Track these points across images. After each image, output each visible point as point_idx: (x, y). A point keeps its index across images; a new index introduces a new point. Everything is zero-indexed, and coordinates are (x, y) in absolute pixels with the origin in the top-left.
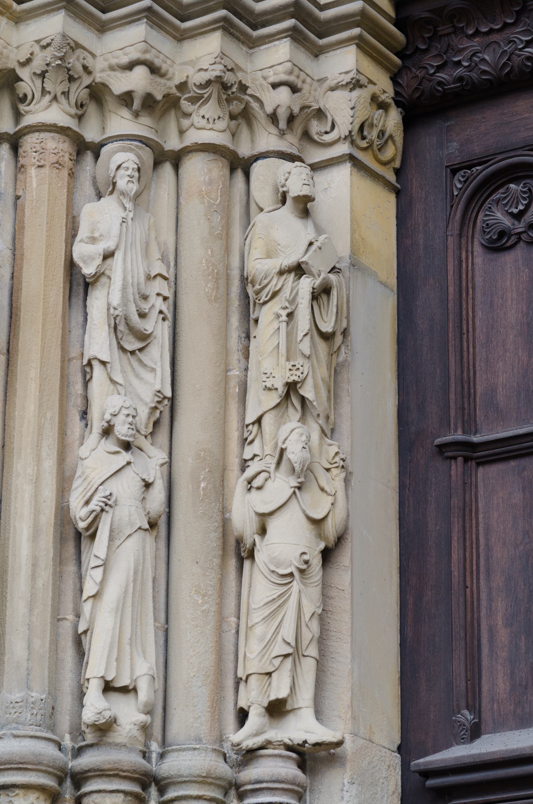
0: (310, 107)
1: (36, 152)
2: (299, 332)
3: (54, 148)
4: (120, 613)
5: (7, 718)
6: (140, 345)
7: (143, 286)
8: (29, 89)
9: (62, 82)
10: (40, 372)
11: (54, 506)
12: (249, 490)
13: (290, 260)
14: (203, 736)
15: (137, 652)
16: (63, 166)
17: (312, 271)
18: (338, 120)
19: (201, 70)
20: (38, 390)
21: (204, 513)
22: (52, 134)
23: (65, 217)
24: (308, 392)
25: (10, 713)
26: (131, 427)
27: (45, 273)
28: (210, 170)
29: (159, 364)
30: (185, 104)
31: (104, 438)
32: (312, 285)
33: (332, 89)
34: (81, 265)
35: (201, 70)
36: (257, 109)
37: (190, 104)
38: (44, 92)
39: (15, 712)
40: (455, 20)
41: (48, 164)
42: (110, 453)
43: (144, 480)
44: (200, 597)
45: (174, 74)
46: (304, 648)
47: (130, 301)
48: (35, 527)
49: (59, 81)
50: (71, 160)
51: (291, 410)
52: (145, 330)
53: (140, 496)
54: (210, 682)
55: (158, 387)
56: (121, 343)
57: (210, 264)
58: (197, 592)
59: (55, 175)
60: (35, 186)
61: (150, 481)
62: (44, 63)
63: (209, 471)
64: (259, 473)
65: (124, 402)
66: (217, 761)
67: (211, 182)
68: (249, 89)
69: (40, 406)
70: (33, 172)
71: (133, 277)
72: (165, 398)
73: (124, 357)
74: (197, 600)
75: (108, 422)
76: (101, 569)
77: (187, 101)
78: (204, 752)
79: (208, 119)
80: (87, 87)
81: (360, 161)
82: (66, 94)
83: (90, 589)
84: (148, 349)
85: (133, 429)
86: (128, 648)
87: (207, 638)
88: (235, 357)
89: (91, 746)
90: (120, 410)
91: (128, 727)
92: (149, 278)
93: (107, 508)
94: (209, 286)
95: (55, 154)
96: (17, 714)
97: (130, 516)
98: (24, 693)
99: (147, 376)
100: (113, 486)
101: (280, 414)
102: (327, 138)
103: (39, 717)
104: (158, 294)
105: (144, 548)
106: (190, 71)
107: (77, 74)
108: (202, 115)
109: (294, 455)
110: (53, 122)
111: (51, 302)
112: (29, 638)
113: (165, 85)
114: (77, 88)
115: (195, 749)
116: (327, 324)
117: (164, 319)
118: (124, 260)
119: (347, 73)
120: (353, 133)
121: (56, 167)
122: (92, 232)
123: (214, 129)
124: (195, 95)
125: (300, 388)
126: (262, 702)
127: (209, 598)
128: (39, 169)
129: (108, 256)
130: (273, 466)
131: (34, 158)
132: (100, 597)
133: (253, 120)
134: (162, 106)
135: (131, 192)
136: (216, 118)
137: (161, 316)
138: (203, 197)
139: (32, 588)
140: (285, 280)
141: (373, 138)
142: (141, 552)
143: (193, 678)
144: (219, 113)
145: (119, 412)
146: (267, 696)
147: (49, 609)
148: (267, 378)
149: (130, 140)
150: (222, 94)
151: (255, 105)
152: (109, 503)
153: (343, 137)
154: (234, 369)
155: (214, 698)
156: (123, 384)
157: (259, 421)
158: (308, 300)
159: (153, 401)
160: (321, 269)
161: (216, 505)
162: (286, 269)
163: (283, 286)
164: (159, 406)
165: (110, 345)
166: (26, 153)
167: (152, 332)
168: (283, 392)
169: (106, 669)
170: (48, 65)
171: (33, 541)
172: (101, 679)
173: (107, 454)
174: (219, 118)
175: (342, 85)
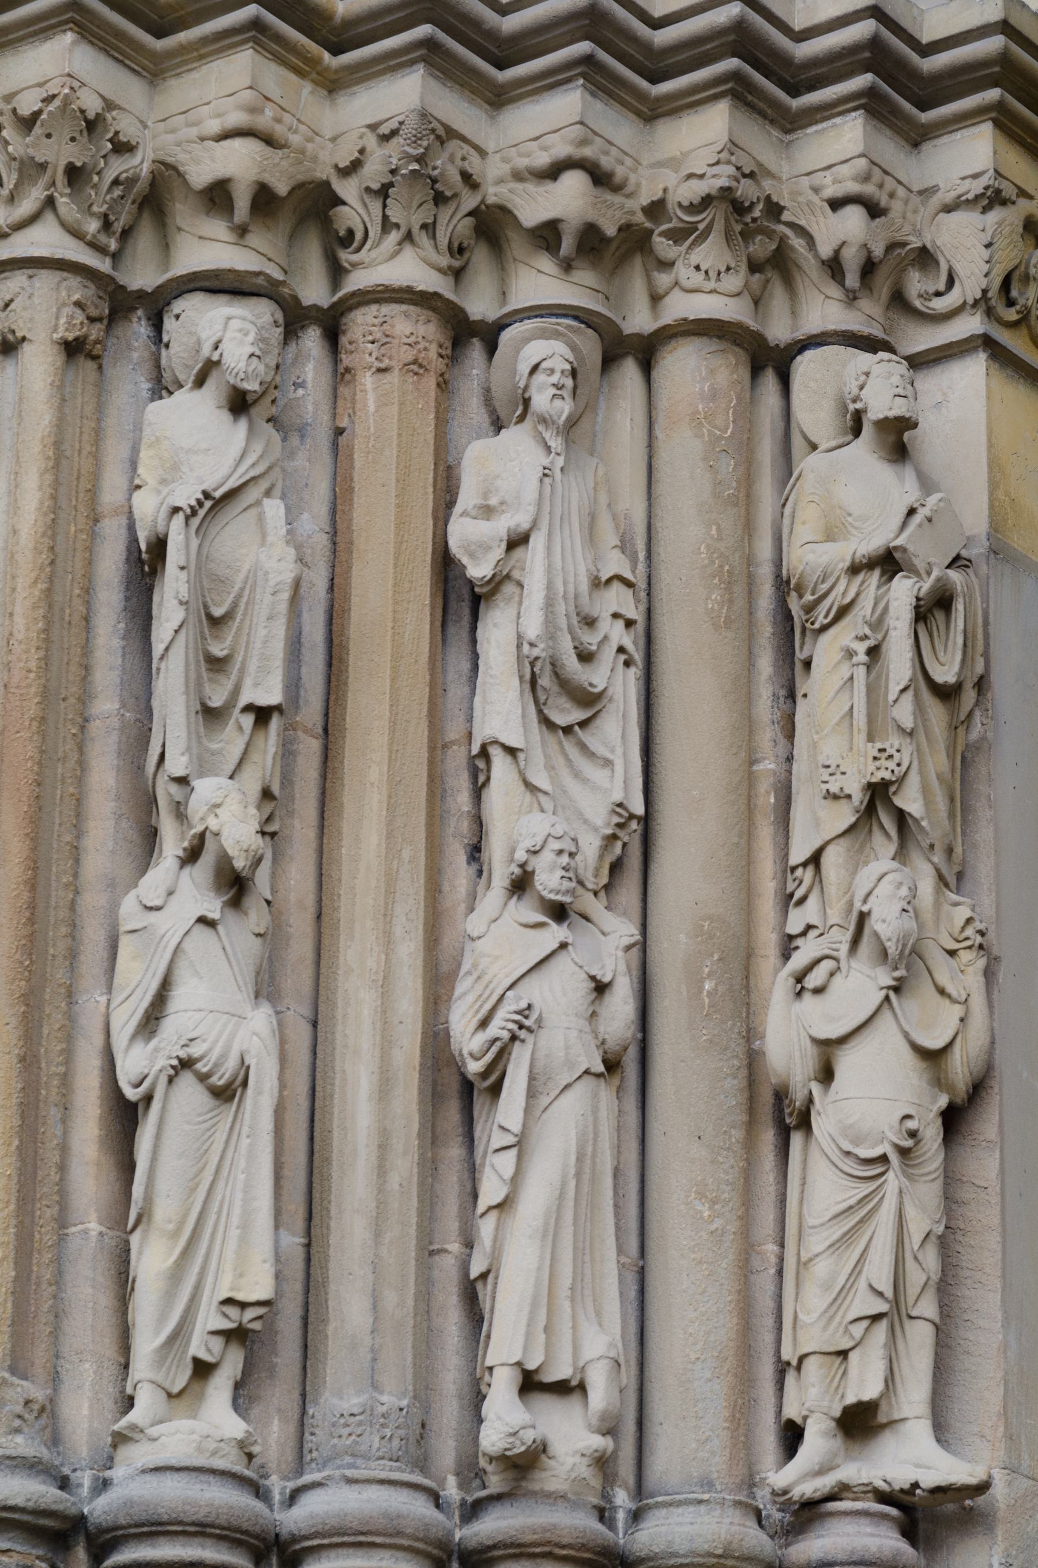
0: (904, 244)
1: (373, 342)
2: (891, 685)
3: (408, 333)
4: (550, 1238)
5: (335, 1446)
6: (579, 715)
7: (585, 600)
8: (358, 220)
9: (421, 205)
10: (389, 771)
11: (420, 1032)
12: (799, 994)
14: (715, 1475)
15: (586, 1315)
16: (426, 369)
17: (914, 565)
18: (960, 269)
19: (691, 176)
20: (385, 805)
21: (711, 1041)
22: (404, 307)
23: (432, 467)
24: (910, 801)
25: (340, 1436)
26: (567, 875)
27: (395, 578)
28: (712, 372)
29: (619, 751)
30: (663, 243)
31: (515, 898)
32: (915, 593)
33: (948, 209)
34: (465, 560)
35: (691, 176)
36: (802, 250)
37: (671, 242)
38: (387, 225)
39: (350, 1435)
42: (526, 926)
43: (593, 978)
44: (707, 1205)
45: (638, 185)
46: (910, 1302)
47: (561, 629)
48: (382, 1073)
49: (415, 204)
50: (441, 356)
51: (878, 837)
52: (591, 685)
53: (587, 1009)
54: (729, 1371)
55: (618, 796)
56: (546, 711)
57: (715, 555)
58: (701, 1195)
60: (372, 407)
61: (606, 979)
62: (387, 169)
63: (720, 960)
64: (818, 961)
66: (744, 1525)
67: (714, 395)
68: (786, 212)
69: (390, 835)
70: (367, 381)
71: (565, 583)
72: (632, 817)
73: (551, 739)
74: (701, 1212)
75: (522, 866)
76: (513, 1152)
77: (665, 237)
78: (718, 1507)
79: (706, 272)
80: (470, 214)
81: (1005, 348)
82: (431, 227)
83: (491, 1191)
84: (598, 722)
85: (570, 879)
86: (567, 1305)
87: (722, 1285)
88: (767, 735)
89: (498, 1498)
91: (570, 1461)
92: (598, 584)
93: (523, 1034)
94: (713, 597)
95: (410, 345)
96: (353, 1437)
97: (567, 1048)
98: (366, 1396)
99: (597, 774)
100: (533, 991)
101: (857, 846)
102: (940, 305)
103: (396, 1443)
104: (616, 616)
105: (595, 1111)
106: (670, 179)
107: (450, 188)
108: (696, 264)
109: (885, 926)
110: (405, 284)
111: (407, 634)
112: (374, 1290)
113: (622, 207)
114: (451, 217)
115: (700, 1502)
116: (946, 667)
117: (627, 664)
118: (549, 549)
119: (975, 176)
120: (990, 295)
122: (486, 495)
123: (719, 290)
124: (681, 225)
125: (894, 793)
126: (830, 1408)
127: (723, 1207)
128: (380, 376)
129: (517, 541)
130: (845, 948)
131: (370, 354)
132: (511, 1207)
134: (618, 248)
135: (559, 417)
136: (723, 269)
137: (622, 657)
138: (700, 423)
139: (380, 1191)
140: (863, 582)
141: (1030, 303)
142: (590, 1119)
143: (694, 1363)
144: (728, 258)
145: (542, 847)
146: (839, 1396)
147: (413, 1231)
148: (831, 775)
149: (557, 316)
150: (733, 222)
151: (797, 243)
152: (527, 1023)
153: (971, 301)
154: (765, 759)
155: (736, 1401)
157: (815, 860)
158: (908, 621)
159: (609, 824)
160: (932, 560)
162: (865, 561)
163: (858, 595)
164: (621, 833)
165: (524, 716)
167: (605, 689)
168: (862, 802)
169: (526, 1349)
170: (393, 172)
171: (380, 1099)
172: (515, 1367)
174: (728, 269)
175: (967, 200)
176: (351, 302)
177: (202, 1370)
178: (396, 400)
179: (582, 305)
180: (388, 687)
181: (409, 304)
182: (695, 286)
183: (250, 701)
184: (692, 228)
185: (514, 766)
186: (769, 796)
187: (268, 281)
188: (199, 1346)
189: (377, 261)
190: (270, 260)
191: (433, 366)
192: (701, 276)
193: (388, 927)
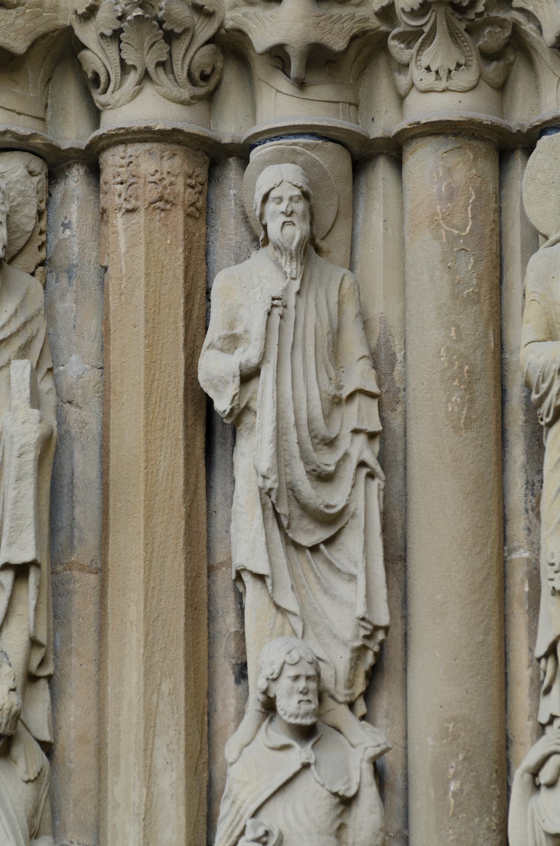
1: (122, 183)
3: (152, 171)
6: (323, 534)
7: (320, 423)
8: (99, 64)
9: (152, 46)
12: (537, 787)
16: (173, 204)
20: (142, 643)
22: (148, 146)
23: (182, 301)
26: (305, 698)
27: (147, 418)
28: (449, 171)
29: (361, 565)
30: (396, 46)
31: (267, 721)
37: (402, 46)
38: (125, 68)
41: (142, 205)
42: (274, 749)
43: (336, 794)
47: (294, 457)
49: (146, 46)
50: (192, 187)
52: (328, 506)
53: (332, 824)
55: (361, 611)
56: (290, 535)
57: (455, 357)
59: (158, 224)
60: (123, 249)
61: (350, 793)
62: (114, 16)
63: (465, 759)
65: (289, 653)
67: (451, 194)
69: (148, 672)
71: (296, 412)
72: (376, 628)
77: (398, 39)
79: (437, 72)
80: (207, 42)
82: (168, 64)
85: (309, 701)
90: (282, 669)
94: (453, 399)
95: (155, 183)
104: (356, 432)
107: (179, 25)
108: (426, 66)
110: (143, 126)
111: (161, 472)
114: (187, 50)
117: (371, 476)
118: (278, 382)
121: (158, 208)
122: (232, 325)
123: (451, 88)
124: (409, 29)
128: (130, 216)
131: (120, 196)
133: (534, 55)
134: (358, 54)
135: (291, 244)
136: (453, 67)
137: (364, 471)
138: (439, 225)
145: (280, 674)
149: (295, 135)
150: (456, 22)
151: (528, 27)
154: (520, 547)
156: (298, 612)
159: (357, 637)
161: (481, 821)
165: (268, 543)
166: (107, 186)
170: (121, 18)
173: (270, 752)
174: (459, 65)
176: (101, 144)
178: (143, 241)
179: (315, 123)
180: (143, 527)
181: (152, 142)
182: (428, 87)
183: (6, 560)
184: (416, 33)
185: (263, 591)
186: (524, 584)
187: (15, 138)
189: (120, 104)
190: (19, 114)
191: (180, 199)
192: (432, 76)
193: (148, 761)
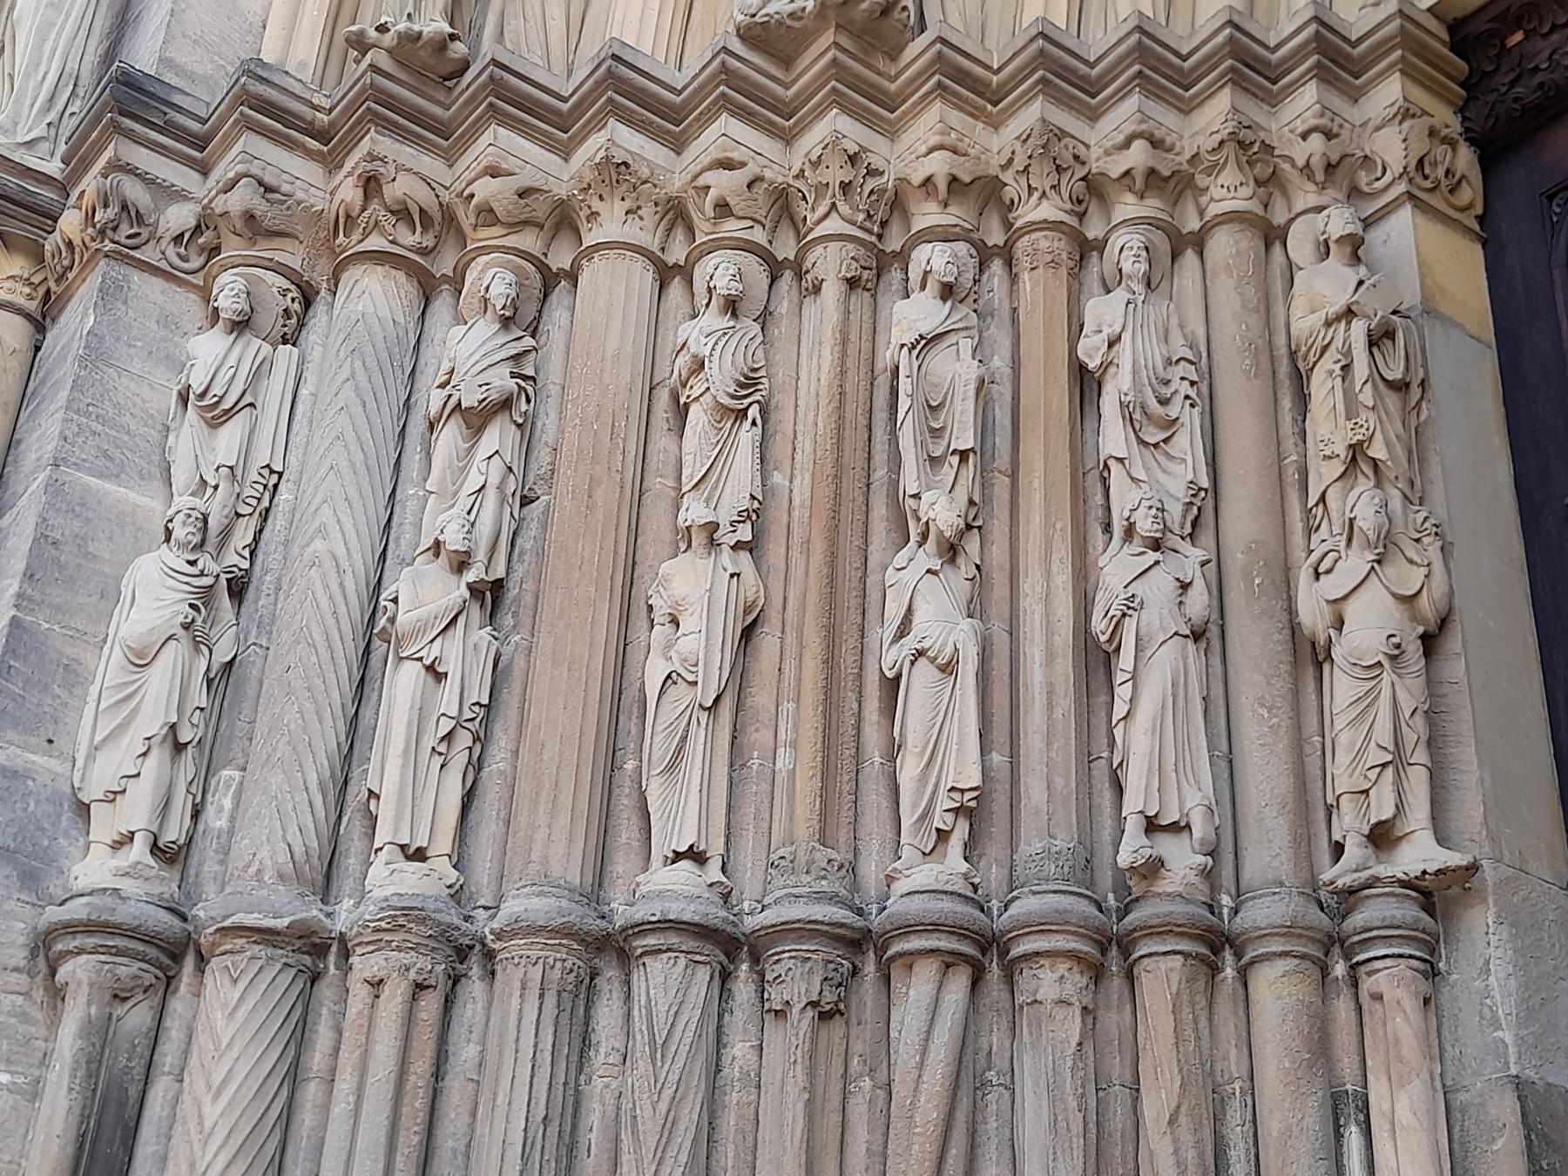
13: (1338, 305)
18: (1388, 159)
24: (1378, 451)
29: (1189, 452)
33: (1378, 129)
34: (1087, 361)
40: (1525, 22)
43: (1178, 579)
46: (1408, 755)
51: (1361, 478)
55: (1190, 477)
58: (1262, 705)
70: (1025, 276)
71: (1145, 360)
72: (1200, 489)
73: (1147, 453)
75: (1128, 519)
84: (1175, 439)
88: (1290, 443)
92: (1169, 362)
93: (1130, 612)
102: (1378, 185)
104: (1183, 379)
105: (1185, 658)
117: (1192, 406)
130: (1343, 544)
137: (1188, 402)
147: (1073, 742)
157: (1323, 498)
163: (1332, 338)
165: (1126, 439)
167: (1177, 418)
177: (943, 835)
188: (940, 820)
